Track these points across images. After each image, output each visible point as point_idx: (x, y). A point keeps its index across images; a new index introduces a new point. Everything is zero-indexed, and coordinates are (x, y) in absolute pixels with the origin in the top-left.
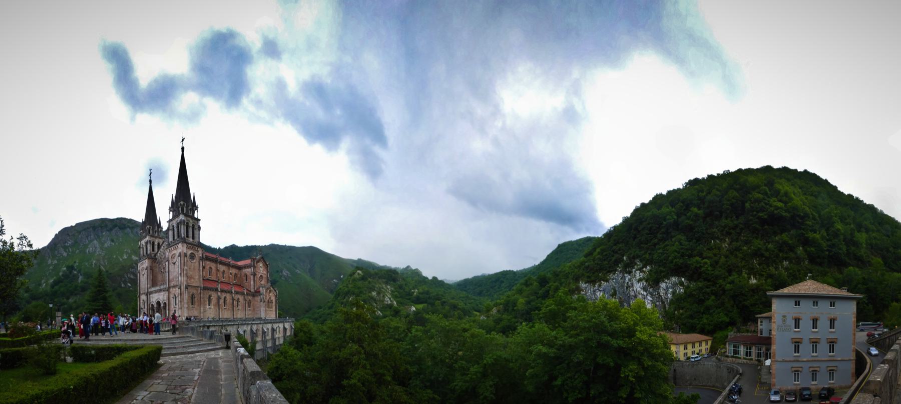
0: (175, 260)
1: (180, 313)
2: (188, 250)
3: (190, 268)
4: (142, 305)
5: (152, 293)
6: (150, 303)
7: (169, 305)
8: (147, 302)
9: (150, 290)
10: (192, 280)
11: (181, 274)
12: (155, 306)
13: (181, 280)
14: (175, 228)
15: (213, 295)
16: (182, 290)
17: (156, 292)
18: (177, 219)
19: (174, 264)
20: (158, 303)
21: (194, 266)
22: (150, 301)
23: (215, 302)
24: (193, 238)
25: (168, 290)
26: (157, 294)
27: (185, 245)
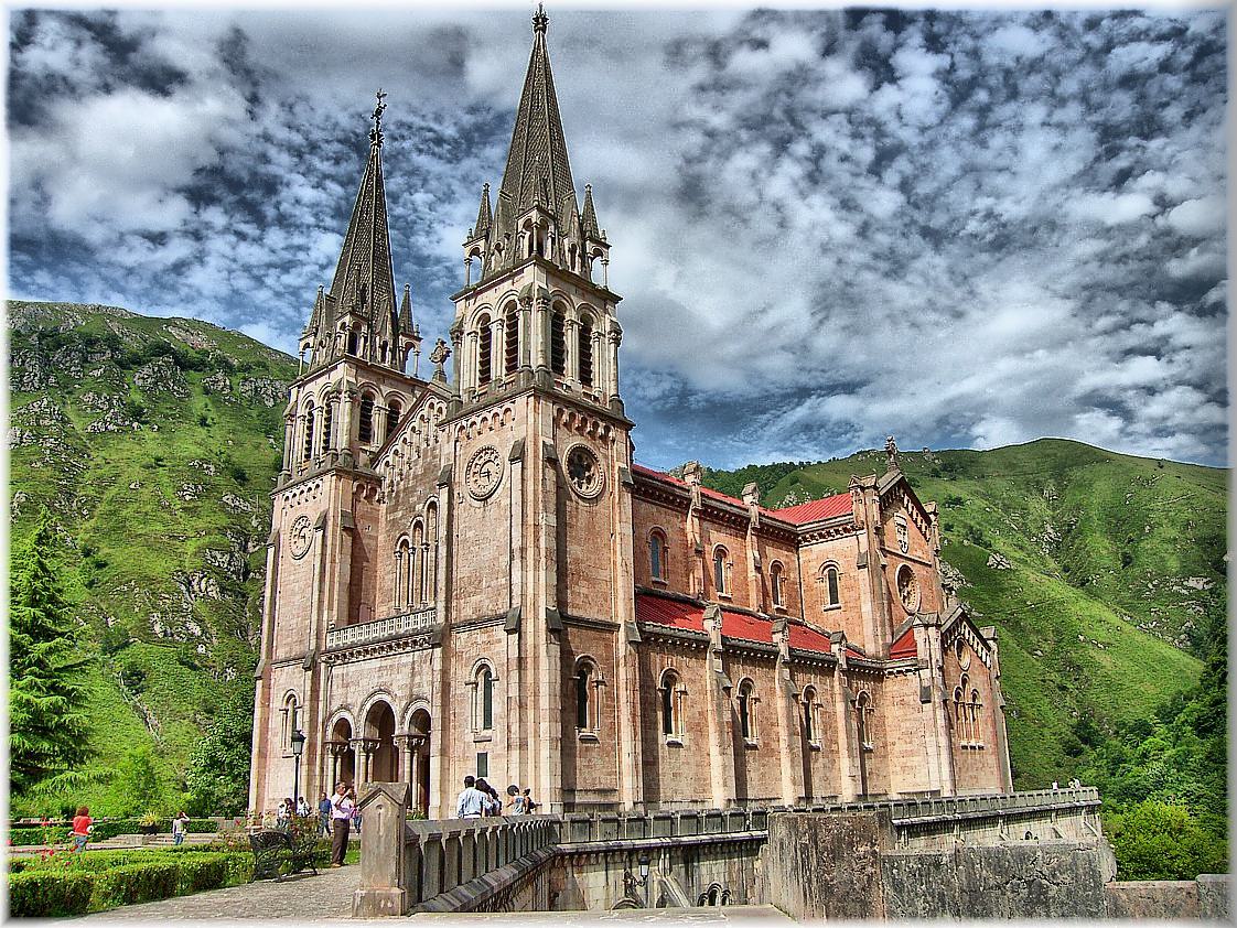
0: (485, 485)
1: (515, 772)
2: (562, 433)
4: (276, 721)
5: (344, 655)
6: (331, 715)
7: (444, 728)
8: (314, 711)
9: (331, 641)
11: (523, 550)
12: (360, 729)
13: (524, 585)
14: (494, 328)
15: (685, 674)
16: (530, 640)
17: (367, 650)
18: (507, 286)
19: (485, 499)
20: (381, 716)
22: (328, 701)
23: (698, 708)
24: (585, 376)
25: (440, 638)
26: (376, 664)
27: (550, 409)
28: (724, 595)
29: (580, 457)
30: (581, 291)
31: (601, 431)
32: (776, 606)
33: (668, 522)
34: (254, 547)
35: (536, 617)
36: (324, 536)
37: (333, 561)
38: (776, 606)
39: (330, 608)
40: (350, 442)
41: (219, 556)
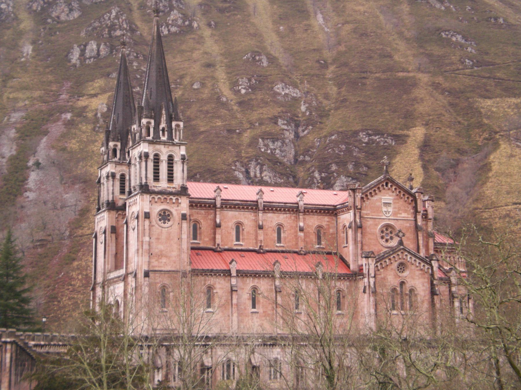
3: (158, 239)
10: (164, 260)
21: (169, 234)
24: (171, 179)
27: (147, 198)
28: (282, 245)
29: (164, 213)
30: (167, 146)
31: (174, 201)
32: (318, 246)
33: (245, 217)
34: (303, 131)
35: (142, 272)
36: (105, 237)
37: (109, 246)
38: (318, 246)
39: (108, 264)
40: (113, 197)
41: (271, 144)
